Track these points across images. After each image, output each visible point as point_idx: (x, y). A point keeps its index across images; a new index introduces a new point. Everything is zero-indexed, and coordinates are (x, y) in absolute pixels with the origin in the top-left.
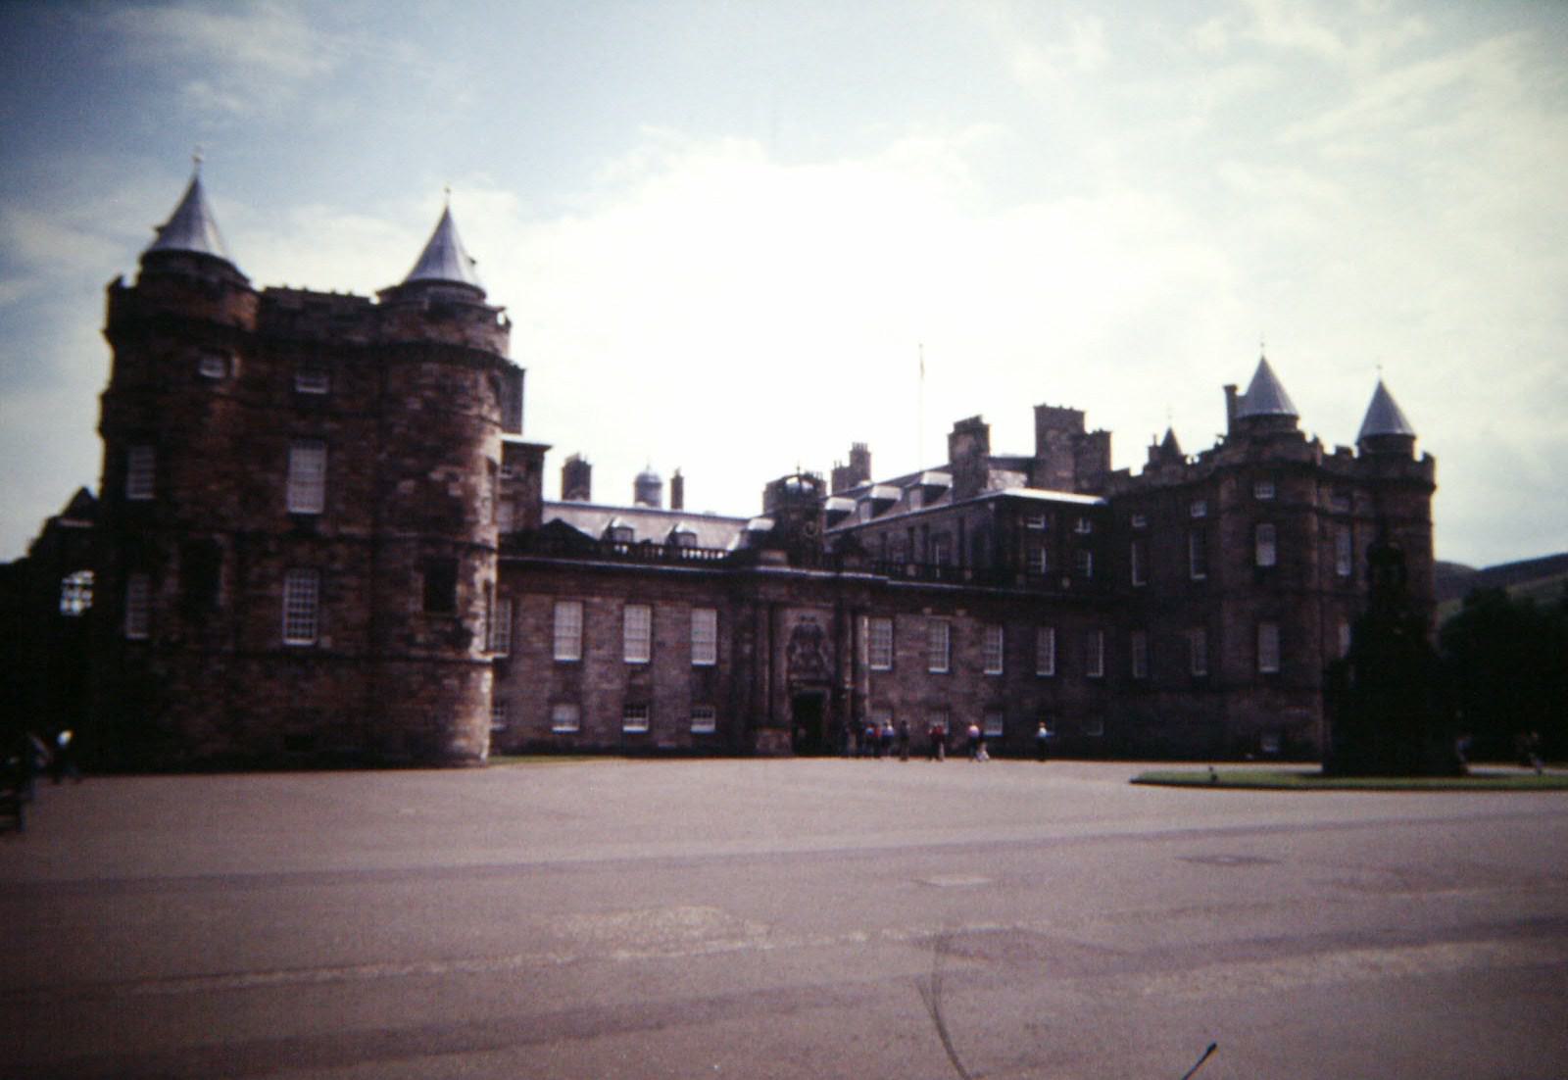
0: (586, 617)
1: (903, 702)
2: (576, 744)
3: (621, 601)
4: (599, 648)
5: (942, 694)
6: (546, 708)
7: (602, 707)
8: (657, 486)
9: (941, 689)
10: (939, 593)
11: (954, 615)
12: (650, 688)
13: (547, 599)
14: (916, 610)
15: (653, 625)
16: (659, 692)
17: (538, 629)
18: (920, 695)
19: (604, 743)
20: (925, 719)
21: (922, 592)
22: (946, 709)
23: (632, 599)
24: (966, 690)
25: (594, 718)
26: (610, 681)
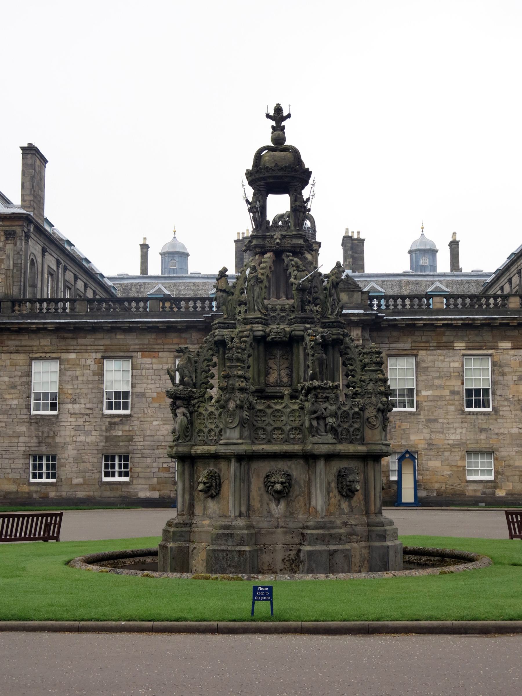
0: (62, 373)
1: (431, 445)
2: (52, 494)
3: (99, 355)
4: (74, 402)
5: (483, 436)
6: (23, 461)
7: (78, 459)
8: (433, 252)
9: (482, 430)
10: (468, 326)
11: (495, 348)
12: (130, 439)
13: (21, 358)
14: (448, 346)
15: (132, 376)
16: (139, 442)
17: (14, 387)
18: (453, 437)
19: (81, 494)
20: (460, 463)
21: (449, 326)
22: (490, 453)
23: (109, 354)
24: (515, 431)
25: (68, 470)
26: (88, 434)
